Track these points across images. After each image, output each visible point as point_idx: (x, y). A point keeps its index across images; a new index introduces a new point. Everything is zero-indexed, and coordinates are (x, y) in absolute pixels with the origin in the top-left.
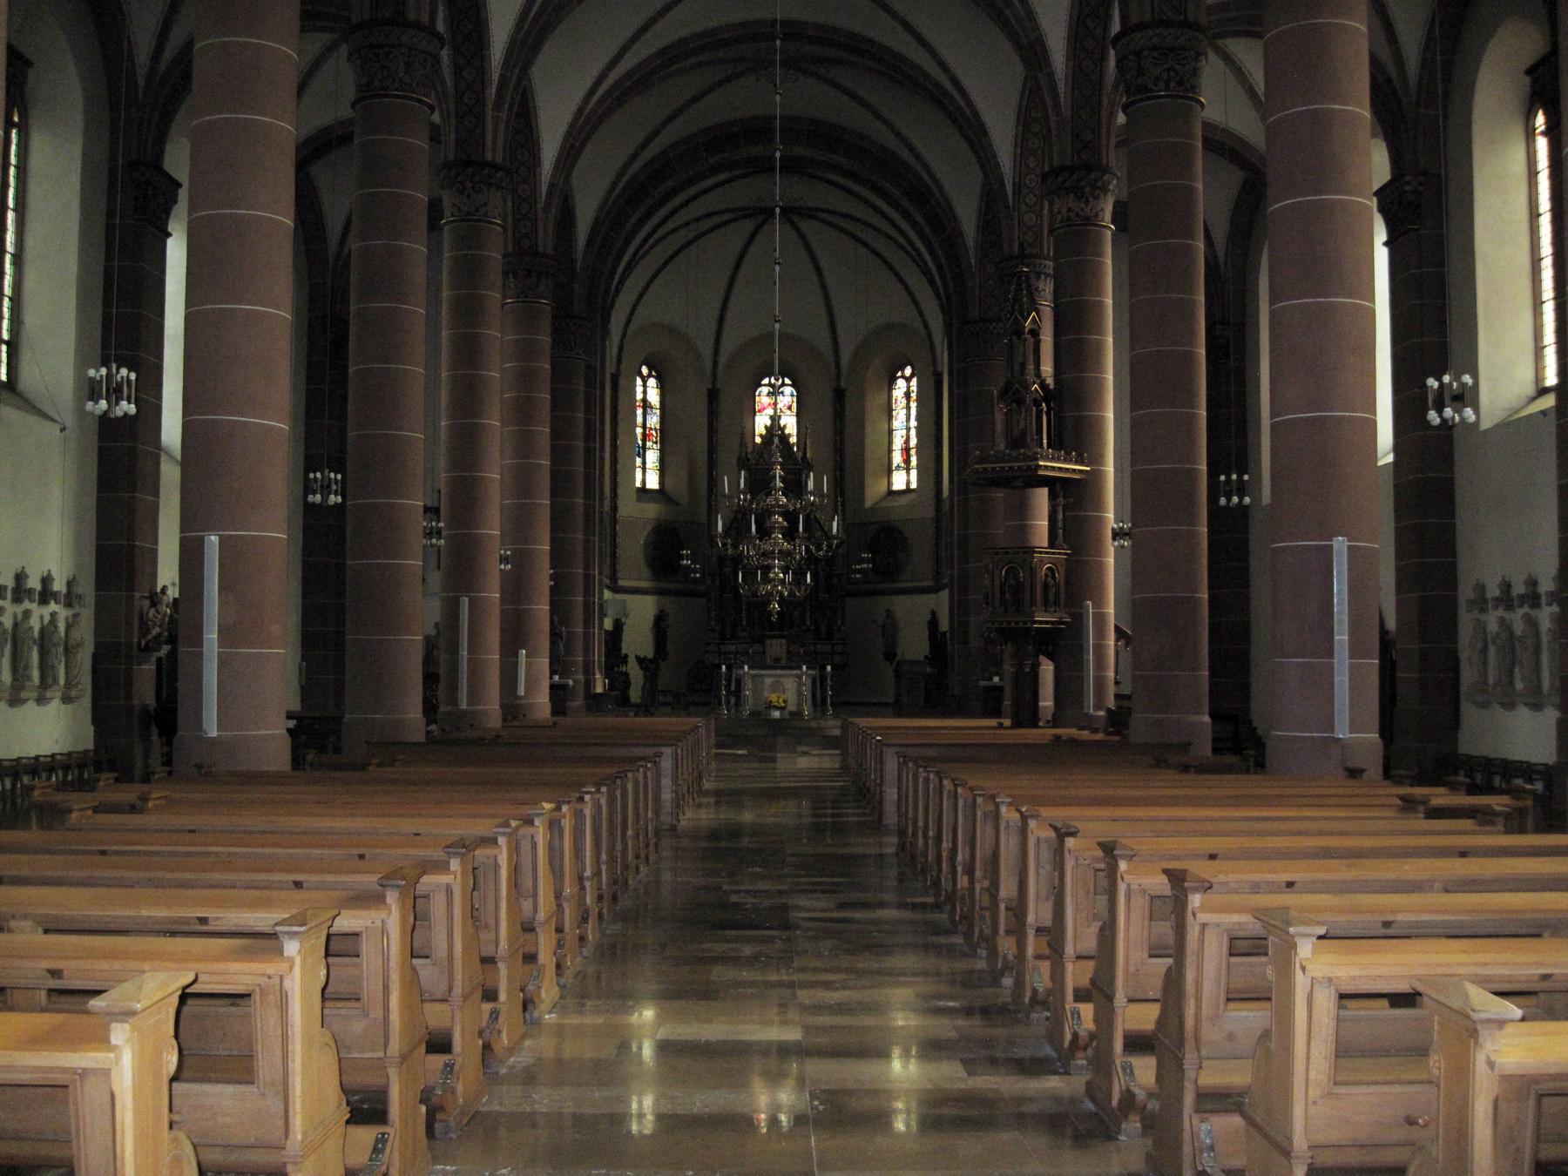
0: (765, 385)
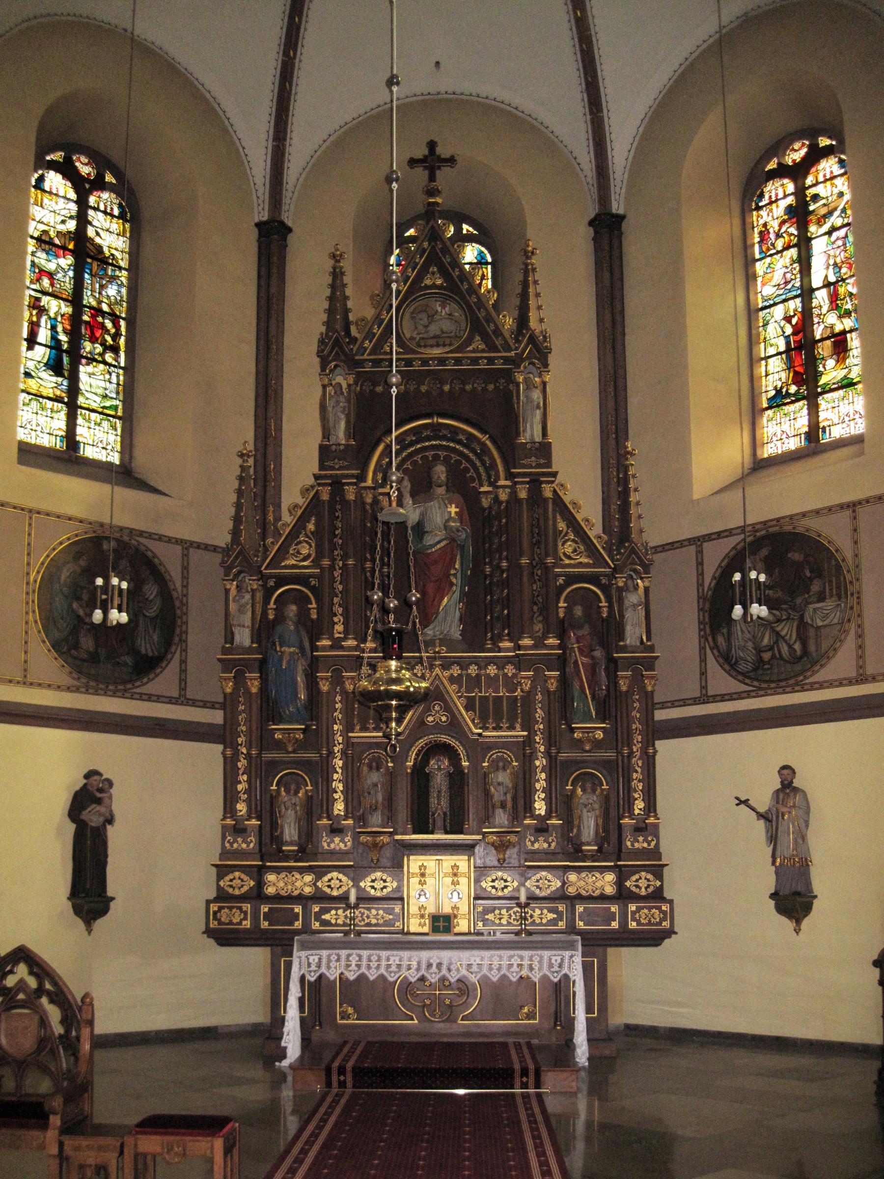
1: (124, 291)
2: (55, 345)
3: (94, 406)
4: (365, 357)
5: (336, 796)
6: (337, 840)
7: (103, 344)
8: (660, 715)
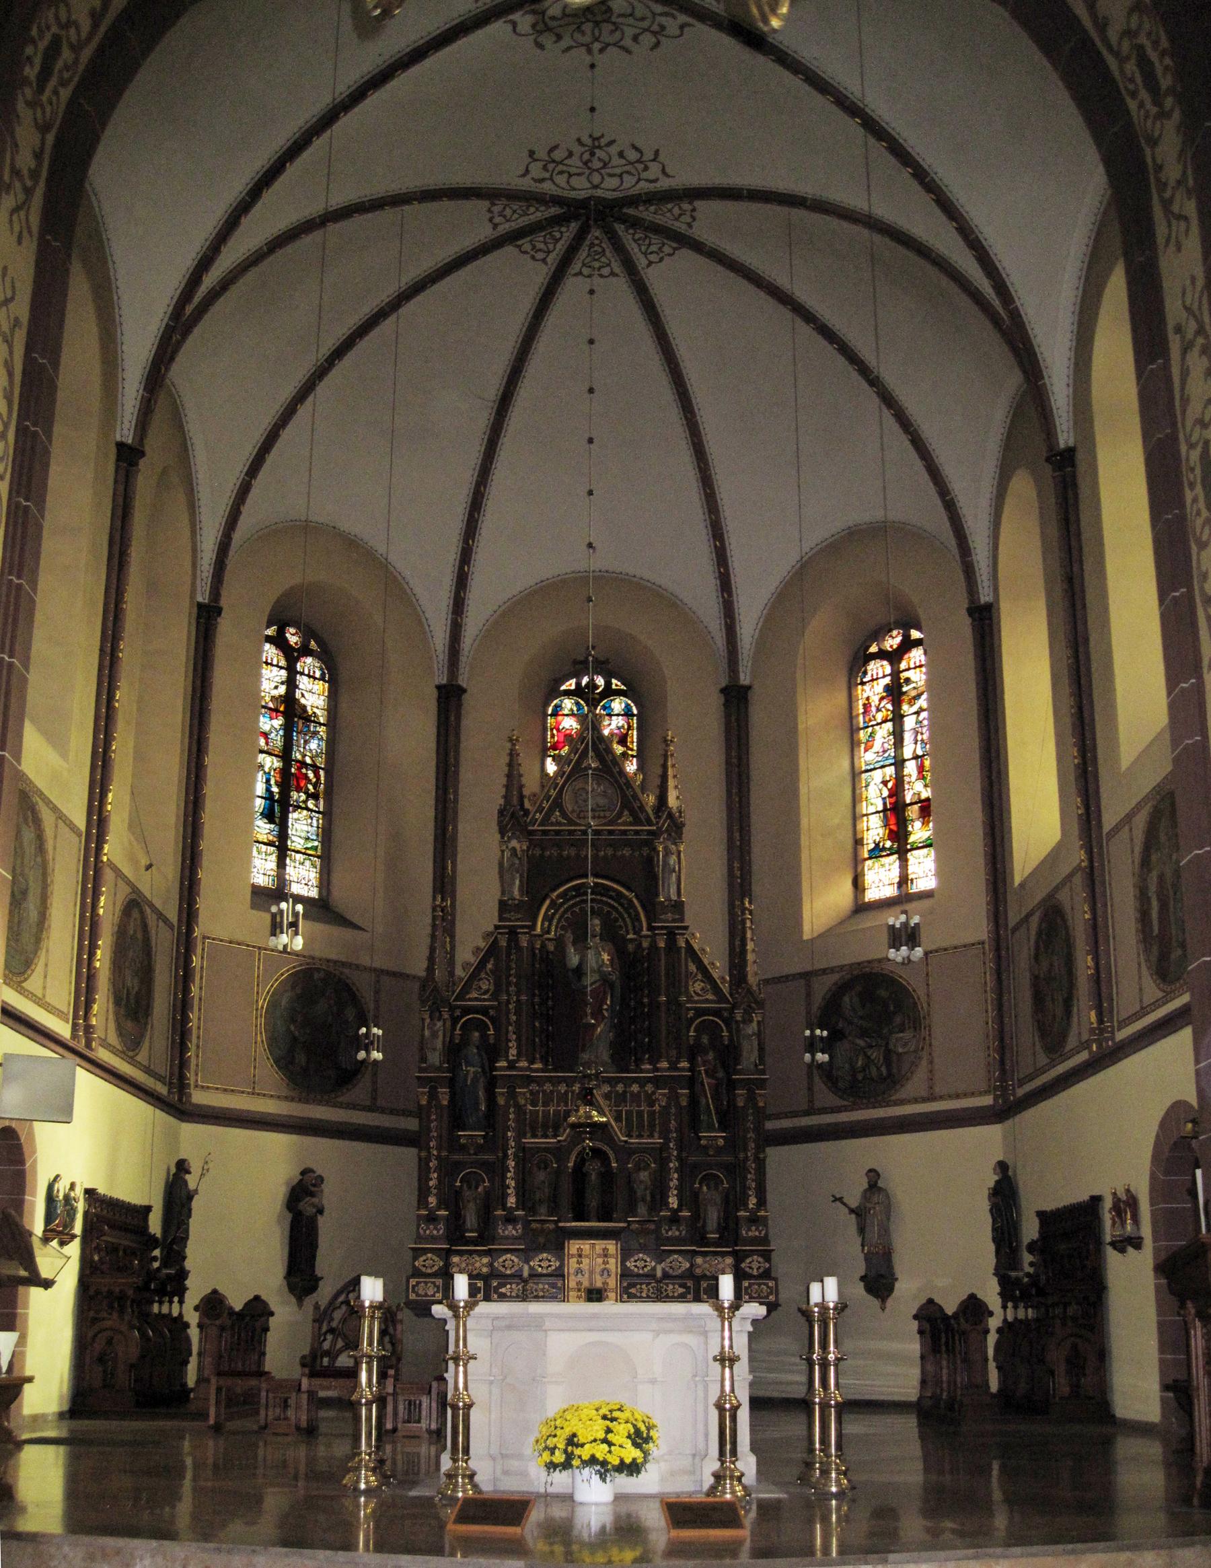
0: (568, 693)
1: (323, 744)
2: (269, 796)
3: (299, 847)
4: (535, 827)
5: (509, 1191)
6: (510, 1227)
7: (306, 793)
8: (770, 1125)
